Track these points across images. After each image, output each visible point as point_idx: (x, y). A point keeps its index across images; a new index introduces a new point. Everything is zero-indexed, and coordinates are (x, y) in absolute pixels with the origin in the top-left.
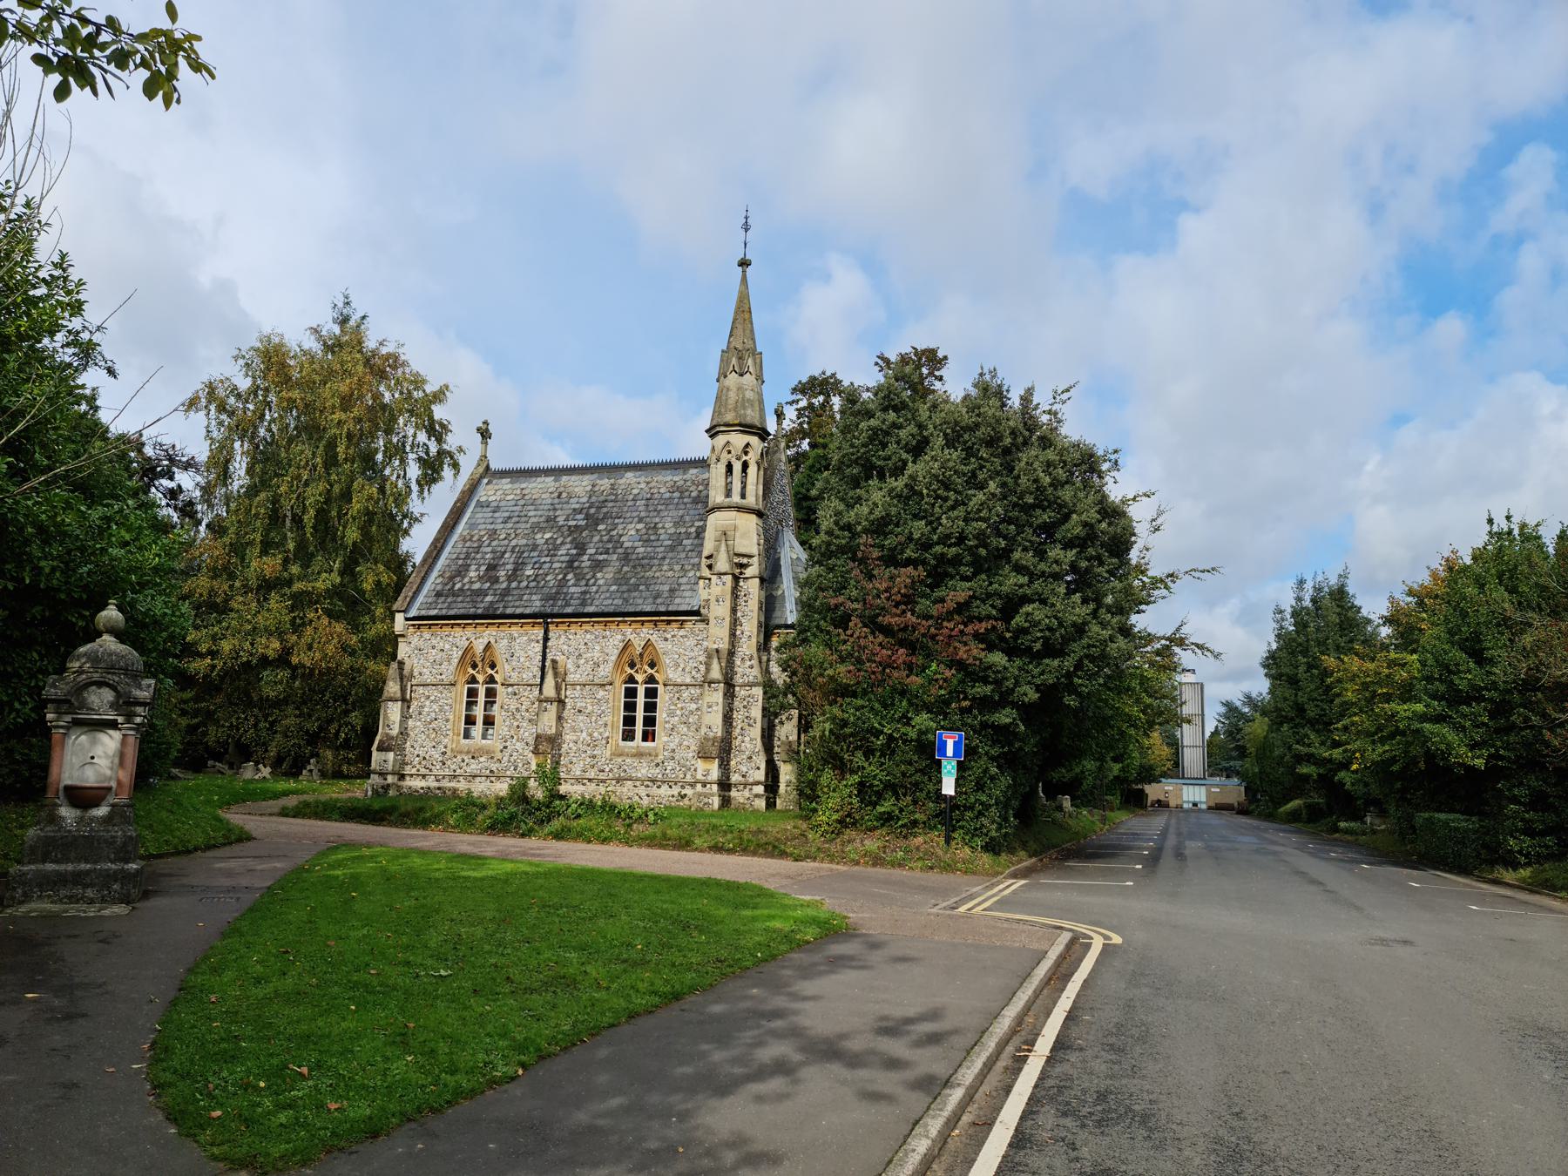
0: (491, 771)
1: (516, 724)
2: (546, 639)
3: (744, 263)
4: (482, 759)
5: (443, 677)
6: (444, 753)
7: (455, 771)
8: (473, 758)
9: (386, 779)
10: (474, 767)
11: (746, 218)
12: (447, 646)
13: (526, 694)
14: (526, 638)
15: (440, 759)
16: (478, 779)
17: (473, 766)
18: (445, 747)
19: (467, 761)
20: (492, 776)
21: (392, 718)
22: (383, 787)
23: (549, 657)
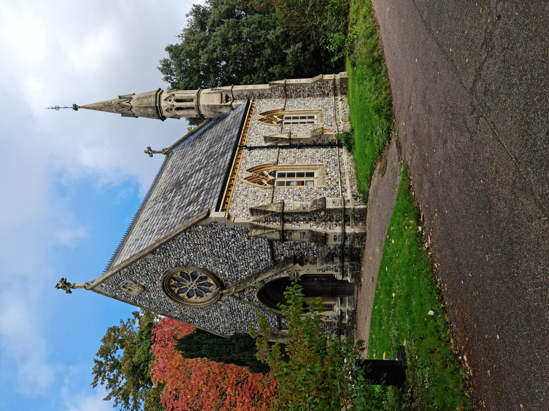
0: (336, 165)
1: (304, 157)
2: (251, 148)
3: (76, 108)
4: (328, 170)
5: (267, 194)
6: (325, 189)
7: (337, 183)
8: (327, 174)
9: (349, 201)
10: (334, 174)
11: (53, 108)
12: (245, 193)
13: (284, 155)
14: (248, 157)
15: (329, 191)
16: (342, 171)
17: (333, 174)
18: (321, 188)
19: (329, 177)
20: (340, 164)
21: (298, 206)
22: (356, 199)
23: (264, 144)
